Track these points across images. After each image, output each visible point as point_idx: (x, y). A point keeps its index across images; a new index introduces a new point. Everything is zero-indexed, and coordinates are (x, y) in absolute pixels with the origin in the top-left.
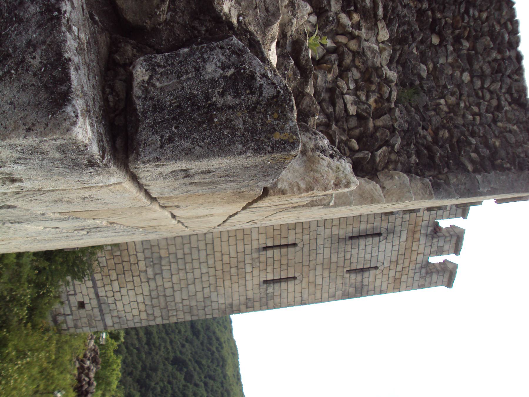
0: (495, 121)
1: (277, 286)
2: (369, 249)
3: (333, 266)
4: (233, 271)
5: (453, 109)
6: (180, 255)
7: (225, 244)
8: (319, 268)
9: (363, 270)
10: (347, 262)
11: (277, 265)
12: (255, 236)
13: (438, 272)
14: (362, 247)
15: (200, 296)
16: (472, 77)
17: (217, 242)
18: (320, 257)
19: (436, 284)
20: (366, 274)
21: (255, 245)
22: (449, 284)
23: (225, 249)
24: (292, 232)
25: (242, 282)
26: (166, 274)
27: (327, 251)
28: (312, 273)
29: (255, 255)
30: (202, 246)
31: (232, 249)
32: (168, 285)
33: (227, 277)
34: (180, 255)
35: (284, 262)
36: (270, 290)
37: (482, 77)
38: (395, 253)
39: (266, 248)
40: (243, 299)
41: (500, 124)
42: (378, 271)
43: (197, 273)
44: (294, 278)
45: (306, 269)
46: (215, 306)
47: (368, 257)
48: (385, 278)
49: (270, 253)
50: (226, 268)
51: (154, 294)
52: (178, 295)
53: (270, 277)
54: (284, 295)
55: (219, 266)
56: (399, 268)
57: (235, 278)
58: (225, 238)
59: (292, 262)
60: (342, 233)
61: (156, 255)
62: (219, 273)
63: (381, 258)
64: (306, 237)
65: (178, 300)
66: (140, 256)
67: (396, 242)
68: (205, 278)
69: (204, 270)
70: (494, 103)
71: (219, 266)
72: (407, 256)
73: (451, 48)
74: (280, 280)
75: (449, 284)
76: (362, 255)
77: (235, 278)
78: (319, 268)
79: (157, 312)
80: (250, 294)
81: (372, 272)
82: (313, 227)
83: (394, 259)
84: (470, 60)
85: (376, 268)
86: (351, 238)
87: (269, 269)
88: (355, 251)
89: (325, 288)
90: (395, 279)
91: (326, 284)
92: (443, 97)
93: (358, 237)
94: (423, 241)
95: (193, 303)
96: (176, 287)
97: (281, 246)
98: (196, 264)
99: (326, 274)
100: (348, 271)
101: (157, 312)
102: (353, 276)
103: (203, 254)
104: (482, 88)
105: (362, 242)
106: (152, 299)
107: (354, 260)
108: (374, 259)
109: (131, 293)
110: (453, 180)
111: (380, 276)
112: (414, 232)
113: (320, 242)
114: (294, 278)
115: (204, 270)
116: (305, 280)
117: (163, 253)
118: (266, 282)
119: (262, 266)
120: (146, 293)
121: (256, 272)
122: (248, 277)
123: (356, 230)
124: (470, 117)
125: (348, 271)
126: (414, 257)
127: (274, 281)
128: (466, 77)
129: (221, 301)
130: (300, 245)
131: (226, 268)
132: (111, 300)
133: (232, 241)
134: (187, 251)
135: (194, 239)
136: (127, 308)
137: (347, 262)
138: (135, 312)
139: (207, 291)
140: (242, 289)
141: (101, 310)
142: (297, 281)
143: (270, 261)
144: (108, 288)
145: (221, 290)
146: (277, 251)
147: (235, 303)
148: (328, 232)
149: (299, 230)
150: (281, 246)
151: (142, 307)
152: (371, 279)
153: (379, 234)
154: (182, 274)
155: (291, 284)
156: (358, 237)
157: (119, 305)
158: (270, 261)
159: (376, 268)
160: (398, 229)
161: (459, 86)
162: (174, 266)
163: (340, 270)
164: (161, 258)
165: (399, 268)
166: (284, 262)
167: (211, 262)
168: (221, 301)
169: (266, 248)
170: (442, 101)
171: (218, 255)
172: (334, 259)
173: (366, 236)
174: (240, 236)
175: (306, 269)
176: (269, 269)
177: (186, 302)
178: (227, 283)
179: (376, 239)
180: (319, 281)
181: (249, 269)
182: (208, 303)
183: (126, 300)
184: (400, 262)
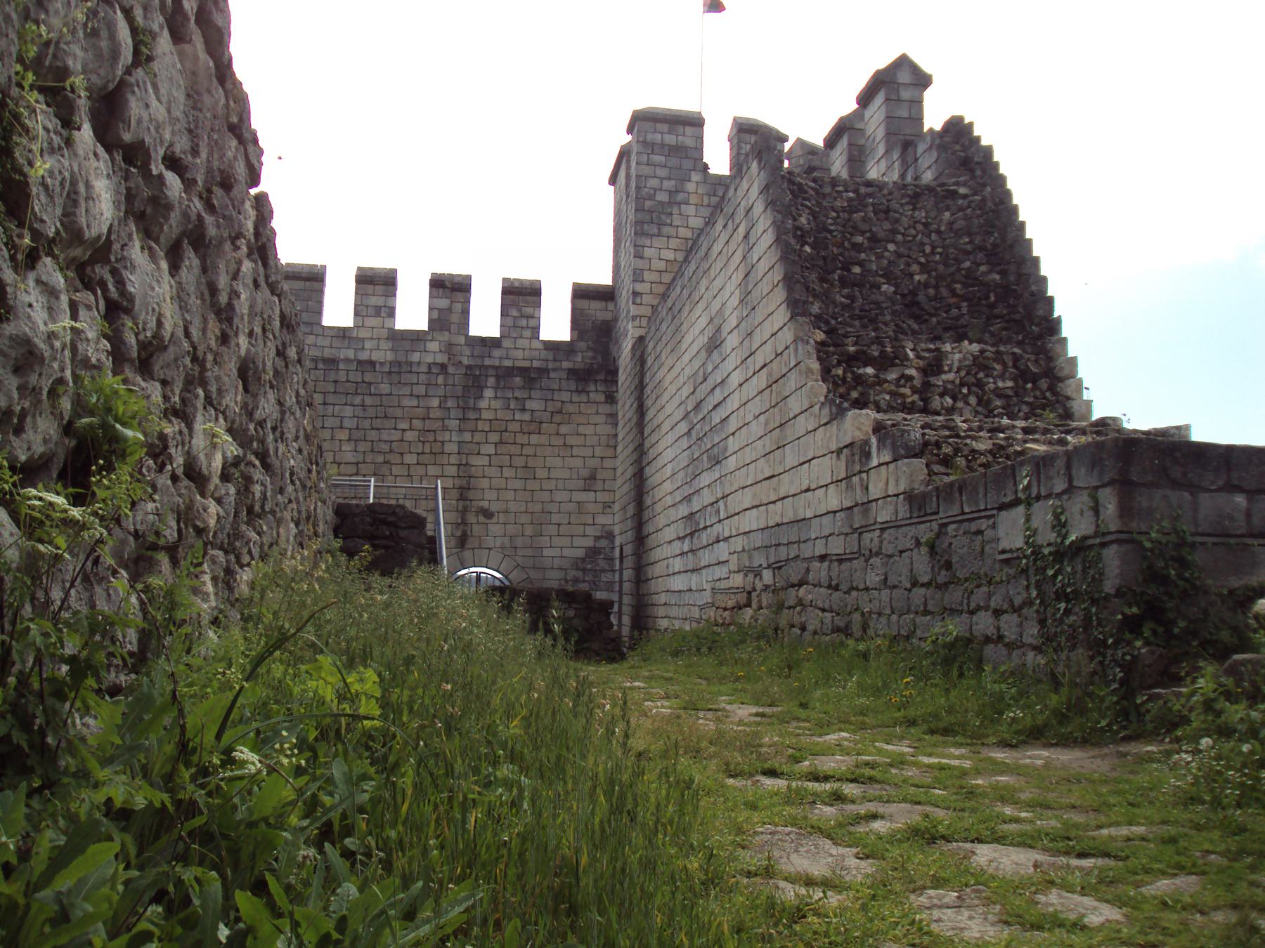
0: (939, 232)
5: (924, 268)
16: (893, 241)
37: (894, 232)
41: (943, 228)
70: (920, 227)
73: (863, 256)
84: (874, 239)
92: (912, 275)
104: (903, 234)
110: (1041, 313)
124: (938, 257)
128: (891, 247)
161: (898, 255)
170: (917, 278)
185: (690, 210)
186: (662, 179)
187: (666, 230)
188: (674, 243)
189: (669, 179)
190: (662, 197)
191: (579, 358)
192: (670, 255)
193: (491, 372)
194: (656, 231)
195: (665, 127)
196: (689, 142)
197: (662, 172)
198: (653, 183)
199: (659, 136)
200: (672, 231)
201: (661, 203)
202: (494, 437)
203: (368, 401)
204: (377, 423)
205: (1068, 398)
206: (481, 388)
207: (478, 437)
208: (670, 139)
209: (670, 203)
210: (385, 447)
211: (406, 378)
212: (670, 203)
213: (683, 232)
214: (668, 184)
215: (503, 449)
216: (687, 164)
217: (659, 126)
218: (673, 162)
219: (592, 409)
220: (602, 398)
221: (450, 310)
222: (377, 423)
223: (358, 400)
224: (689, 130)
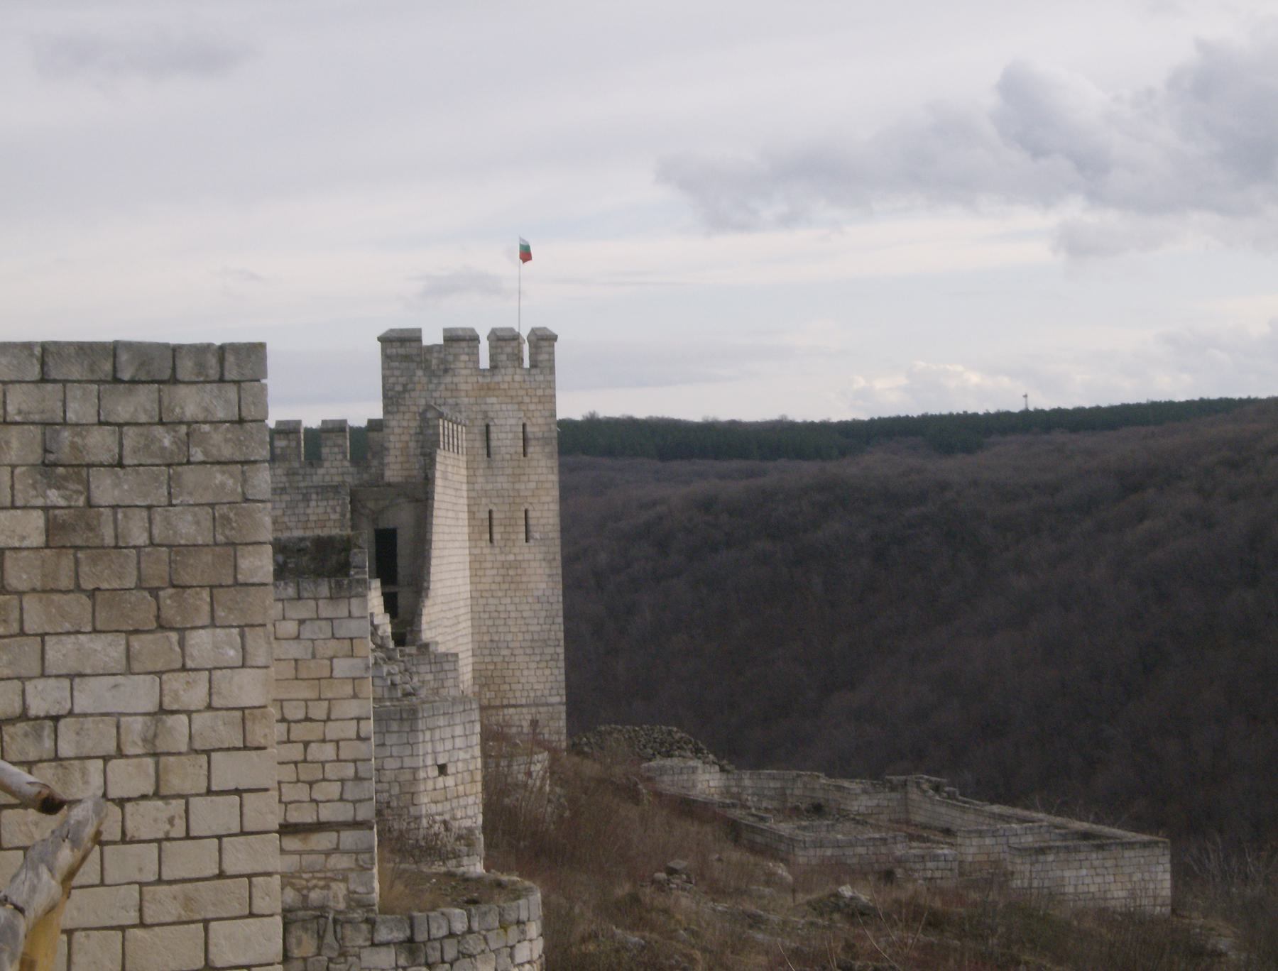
1: (532, 528)
2: (502, 436)
3: (517, 471)
4: (511, 572)
6: (490, 622)
7: (483, 580)
8: (517, 486)
9: (525, 440)
10: (516, 457)
12: (477, 551)
13: (536, 354)
14: (499, 443)
15: (538, 607)
17: (480, 587)
18: (505, 486)
19: (552, 354)
20: (530, 436)
21: (487, 551)
22: (554, 338)
23: (489, 580)
24: (478, 515)
25: (524, 565)
26: (509, 637)
27: (499, 479)
29: (497, 551)
30: (482, 601)
31: (489, 572)
32: (520, 637)
33: (518, 578)
34: (490, 622)
36: (537, 536)
38: (510, 407)
39: (491, 540)
40: (544, 564)
42: (528, 423)
43: (510, 608)
44: (526, 512)
45: (518, 500)
46: (548, 592)
47: (510, 436)
49: (497, 536)
51: (528, 651)
52: (532, 628)
53: (523, 536)
54: (543, 521)
55: (506, 586)
56: (527, 399)
57: (519, 571)
58: (477, 579)
60: (483, 465)
61: (489, 645)
62: (513, 586)
63: (512, 421)
64: (484, 501)
65: (538, 628)
66: (487, 659)
67: (497, 407)
68: (517, 600)
69: (508, 600)
71: (506, 586)
72: (514, 393)
75: (554, 338)
76: (508, 442)
77: (519, 571)
78: (517, 486)
79: (550, 650)
80: (539, 556)
81: (528, 429)
82: (474, 494)
83: (516, 407)
85: (524, 426)
86: (489, 455)
87: (513, 537)
88: (503, 450)
89: (543, 478)
90: (540, 402)
93: (488, 447)
94: (498, 378)
95: (543, 614)
96: (524, 629)
97: (491, 526)
98: (501, 608)
99: (525, 478)
100: (525, 454)
101: (550, 650)
102: (530, 450)
103: (491, 601)
105: (493, 444)
106: (534, 654)
107: (512, 450)
109: (525, 673)
111: (534, 420)
112: (489, 389)
113: (489, 487)
114: (526, 512)
115: (508, 600)
116: (530, 500)
117: (486, 638)
118: (527, 540)
119: (510, 544)
120: (527, 659)
121: (516, 550)
122: (520, 558)
123: (481, 451)
125: (525, 454)
126: (517, 385)
127: (527, 532)
129: (543, 586)
130: (491, 507)
132: (532, 694)
133: (480, 573)
134: (487, 616)
135: (475, 609)
136: (543, 679)
137: (516, 457)
138: (547, 672)
139: (530, 600)
140: (533, 564)
141: (543, 705)
142: (530, 508)
144: (518, 694)
145: (531, 586)
146: (495, 529)
147: (547, 571)
148: (480, 479)
149: (475, 509)
150: (491, 526)
151: (543, 665)
152: (536, 429)
153: (488, 426)
154: (510, 622)
155: (531, 514)
156: (488, 447)
157: (536, 687)
159: (524, 426)
160: (484, 407)
162: (500, 629)
163: (522, 464)
164: (492, 641)
165: (527, 399)
167: (500, 594)
169: (491, 540)
171: (494, 587)
172: (509, 471)
173: (488, 439)
174: (477, 565)
175: (518, 500)
176: (513, 537)
177: (541, 621)
178: (524, 579)
179: (492, 429)
180: (533, 485)
181: (511, 557)
182: (544, 599)
183: (533, 680)
186: (398, 377)
187: (402, 408)
188: (407, 416)
189: (402, 376)
190: (399, 388)
192: (405, 424)
194: (395, 409)
195: (398, 344)
196: (414, 351)
197: (397, 373)
198: (392, 380)
199: (394, 350)
201: (399, 392)
205: (425, 581)
206: (309, 500)
208: (402, 351)
209: (405, 390)
212: (405, 390)
213: (414, 409)
214: (403, 380)
216: (413, 365)
217: (394, 344)
218: (404, 365)
221: (288, 447)
224: (413, 344)
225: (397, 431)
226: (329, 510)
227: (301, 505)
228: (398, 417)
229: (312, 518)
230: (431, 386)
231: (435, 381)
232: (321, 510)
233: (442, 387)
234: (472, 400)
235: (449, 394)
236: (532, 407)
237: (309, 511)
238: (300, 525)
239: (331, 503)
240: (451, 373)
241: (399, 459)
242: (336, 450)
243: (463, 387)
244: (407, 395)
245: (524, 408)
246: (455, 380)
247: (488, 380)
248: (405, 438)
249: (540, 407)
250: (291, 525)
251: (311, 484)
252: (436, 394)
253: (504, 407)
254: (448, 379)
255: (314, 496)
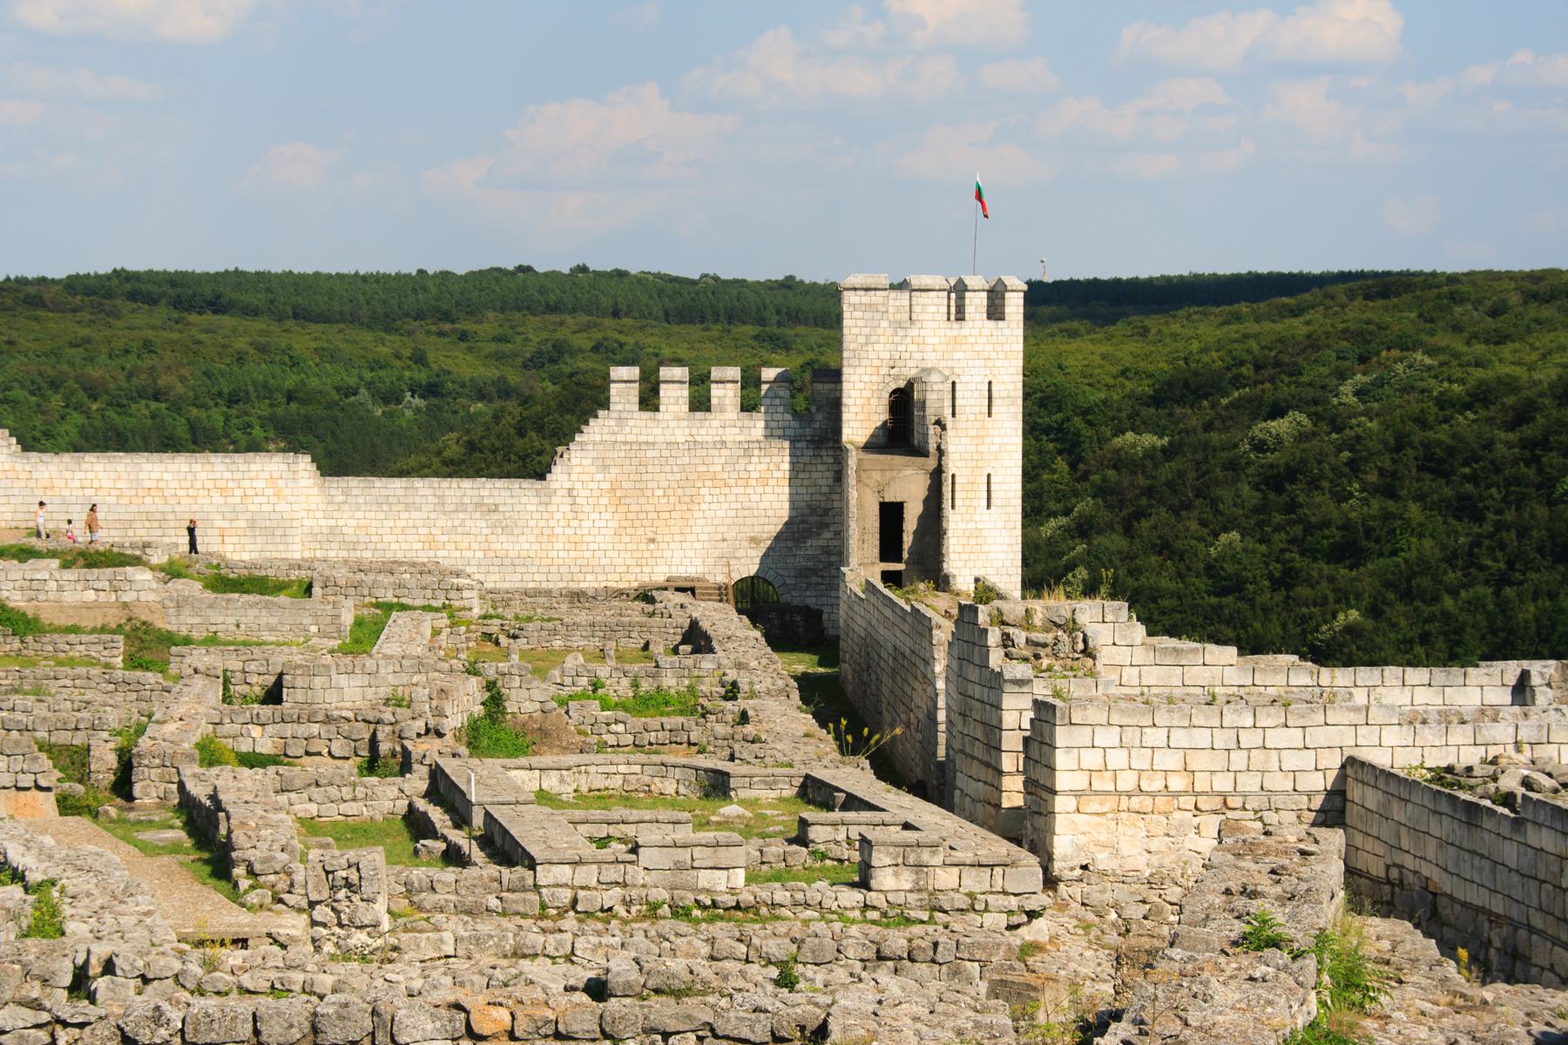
2: (967, 394)
3: (981, 433)
4: (972, 541)
8: (981, 449)
10: (979, 417)
11: (971, 495)
18: (970, 449)
28: (985, 457)
35: (969, 487)
38: (977, 363)
40: (1004, 532)
48: (1003, 371)
50: (968, 549)
54: (1006, 487)
57: (980, 541)
59: (972, 479)
62: (973, 556)
63: (979, 379)
67: (963, 363)
72: (979, 348)
74: (989, 491)
76: (972, 402)
77: (980, 541)
78: (981, 449)
83: (982, 363)
85: (990, 383)
87: (975, 503)
88: (968, 410)
89: (1006, 440)
91: (996, 440)
94: (965, 332)
99: (988, 440)
100: (990, 414)
107: (977, 410)
108: (979, 387)
111: (1000, 378)
118: (989, 506)
119: (971, 510)
121: (976, 517)
122: (980, 526)
125: (990, 414)
127: (989, 498)
131: (968, 549)
143: (968, 502)
158: (968, 502)
159: (990, 383)
160: (950, 363)
165: (994, 355)
166: (969, 487)
168: (1003, 556)
172: (973, 432)
176: (975, 503)
178: (984, 548)
180: (996, 448)
181: (972, 525)
182: (1003, 571)
184: (987, 355)
185: (878, 347)
187: (864, 362)
190: (862, 340)
191: (817, 425)
192: (867, 378)
193: (757, 445)
194: (857, 363)
195: (863, 293)
200: (868, 362)
201: (862, 344)
202: (760, 490)
203: (675, 469)
204: (682, 484)
207: (750, 490)
210: (687, 499)
211: (699, 452)
215: (764, 498)
216: (877, 316)
218: (868, 315)
219: (825, 467)
220: (831, 460)
222: (682, 484)
223: (668, 469)
225: (859, 386)
226: (772, 467)
227: (743, 461)
228: (859, 370)
229: (753, 475)
230: (897, 339)
231: (901, 332)
232: (764, 467)
233: (909, 340)
234: (939, 355)
235: (913, 348)
236: (999, 363)
237: (750, 468)
238: (740, 482)
239: (775, 459)
240: (918, 325)
241: (860, 417)
242: (777, 401)
243: (929, 340)
244: (870, 348)
245: (990, 363)
246: (923, 332)
247: (955, 333)
248: (867, 394)
249: (1007, 363)
250: (732, 482)
251: (749, 438)
252: (901, 348)
253: (970, 363)
254: (915, 332)
255: (756, 452)
